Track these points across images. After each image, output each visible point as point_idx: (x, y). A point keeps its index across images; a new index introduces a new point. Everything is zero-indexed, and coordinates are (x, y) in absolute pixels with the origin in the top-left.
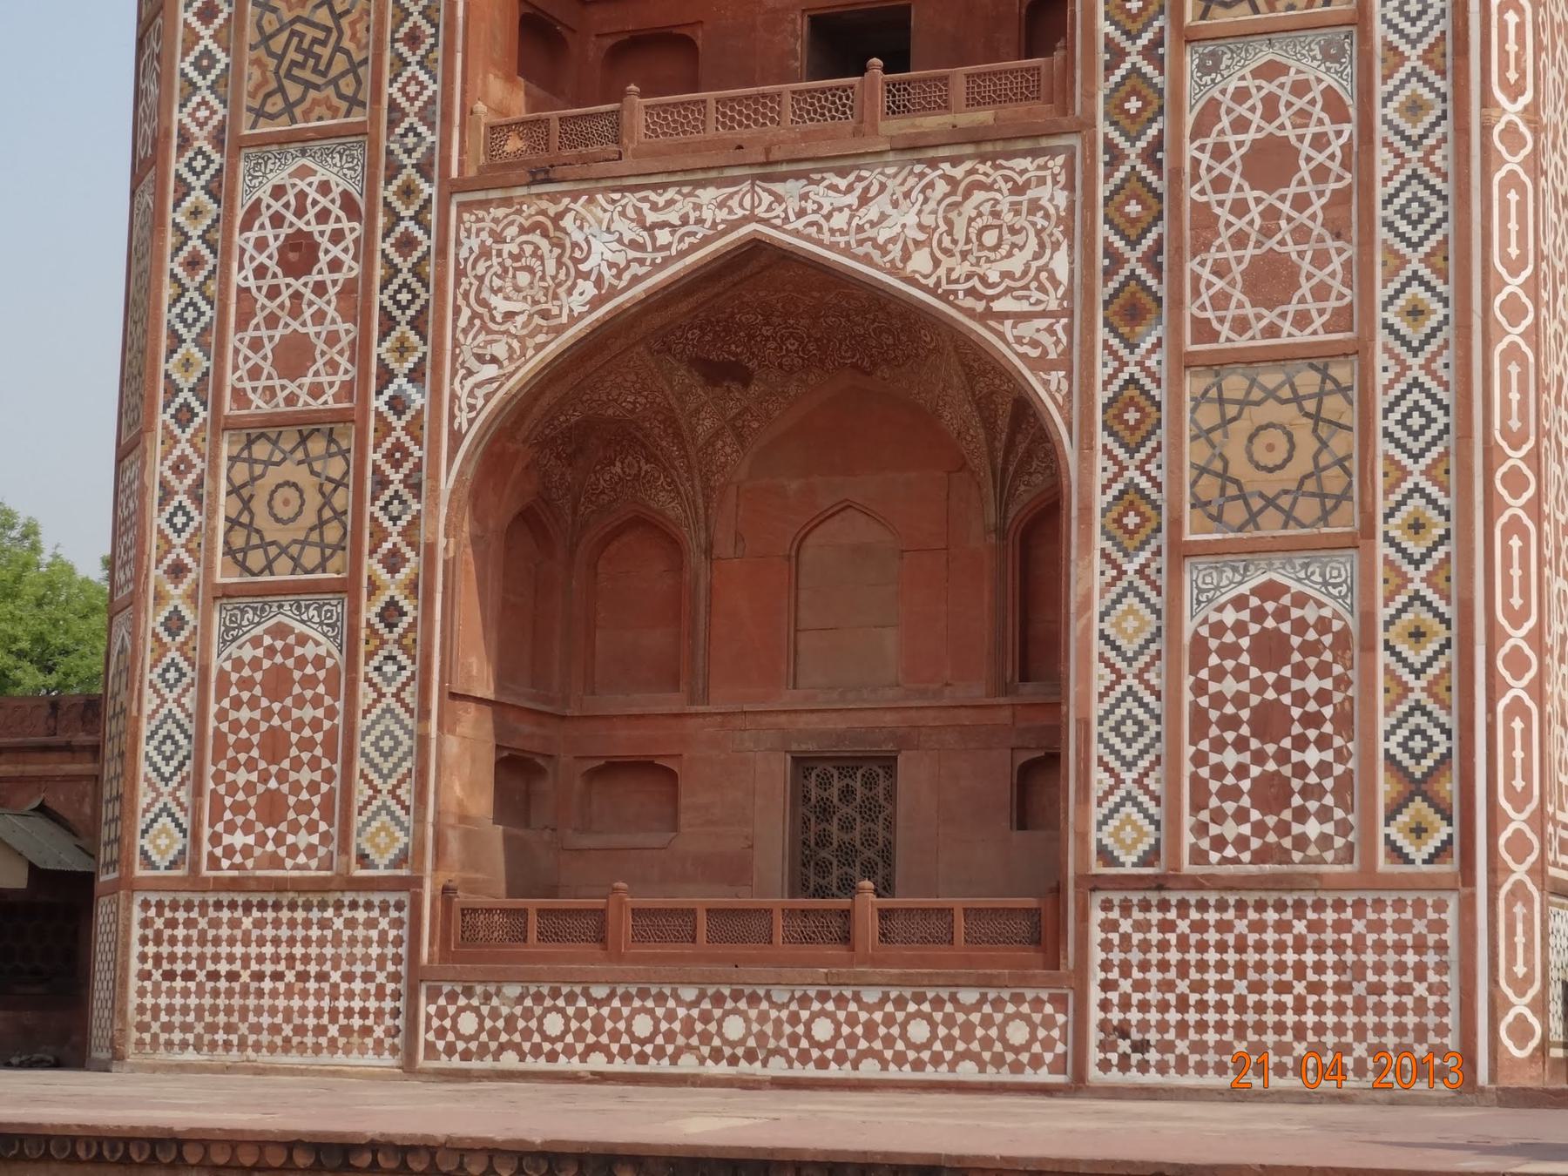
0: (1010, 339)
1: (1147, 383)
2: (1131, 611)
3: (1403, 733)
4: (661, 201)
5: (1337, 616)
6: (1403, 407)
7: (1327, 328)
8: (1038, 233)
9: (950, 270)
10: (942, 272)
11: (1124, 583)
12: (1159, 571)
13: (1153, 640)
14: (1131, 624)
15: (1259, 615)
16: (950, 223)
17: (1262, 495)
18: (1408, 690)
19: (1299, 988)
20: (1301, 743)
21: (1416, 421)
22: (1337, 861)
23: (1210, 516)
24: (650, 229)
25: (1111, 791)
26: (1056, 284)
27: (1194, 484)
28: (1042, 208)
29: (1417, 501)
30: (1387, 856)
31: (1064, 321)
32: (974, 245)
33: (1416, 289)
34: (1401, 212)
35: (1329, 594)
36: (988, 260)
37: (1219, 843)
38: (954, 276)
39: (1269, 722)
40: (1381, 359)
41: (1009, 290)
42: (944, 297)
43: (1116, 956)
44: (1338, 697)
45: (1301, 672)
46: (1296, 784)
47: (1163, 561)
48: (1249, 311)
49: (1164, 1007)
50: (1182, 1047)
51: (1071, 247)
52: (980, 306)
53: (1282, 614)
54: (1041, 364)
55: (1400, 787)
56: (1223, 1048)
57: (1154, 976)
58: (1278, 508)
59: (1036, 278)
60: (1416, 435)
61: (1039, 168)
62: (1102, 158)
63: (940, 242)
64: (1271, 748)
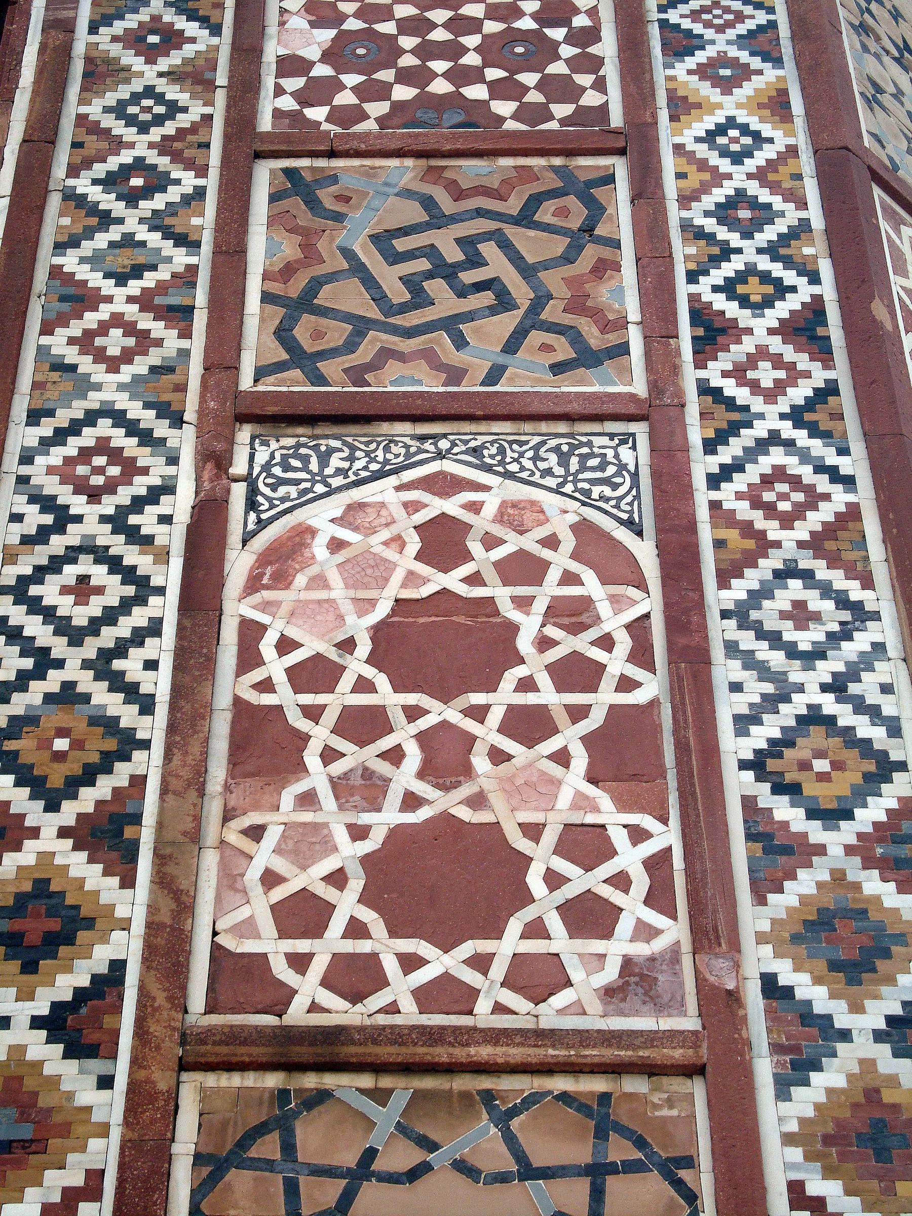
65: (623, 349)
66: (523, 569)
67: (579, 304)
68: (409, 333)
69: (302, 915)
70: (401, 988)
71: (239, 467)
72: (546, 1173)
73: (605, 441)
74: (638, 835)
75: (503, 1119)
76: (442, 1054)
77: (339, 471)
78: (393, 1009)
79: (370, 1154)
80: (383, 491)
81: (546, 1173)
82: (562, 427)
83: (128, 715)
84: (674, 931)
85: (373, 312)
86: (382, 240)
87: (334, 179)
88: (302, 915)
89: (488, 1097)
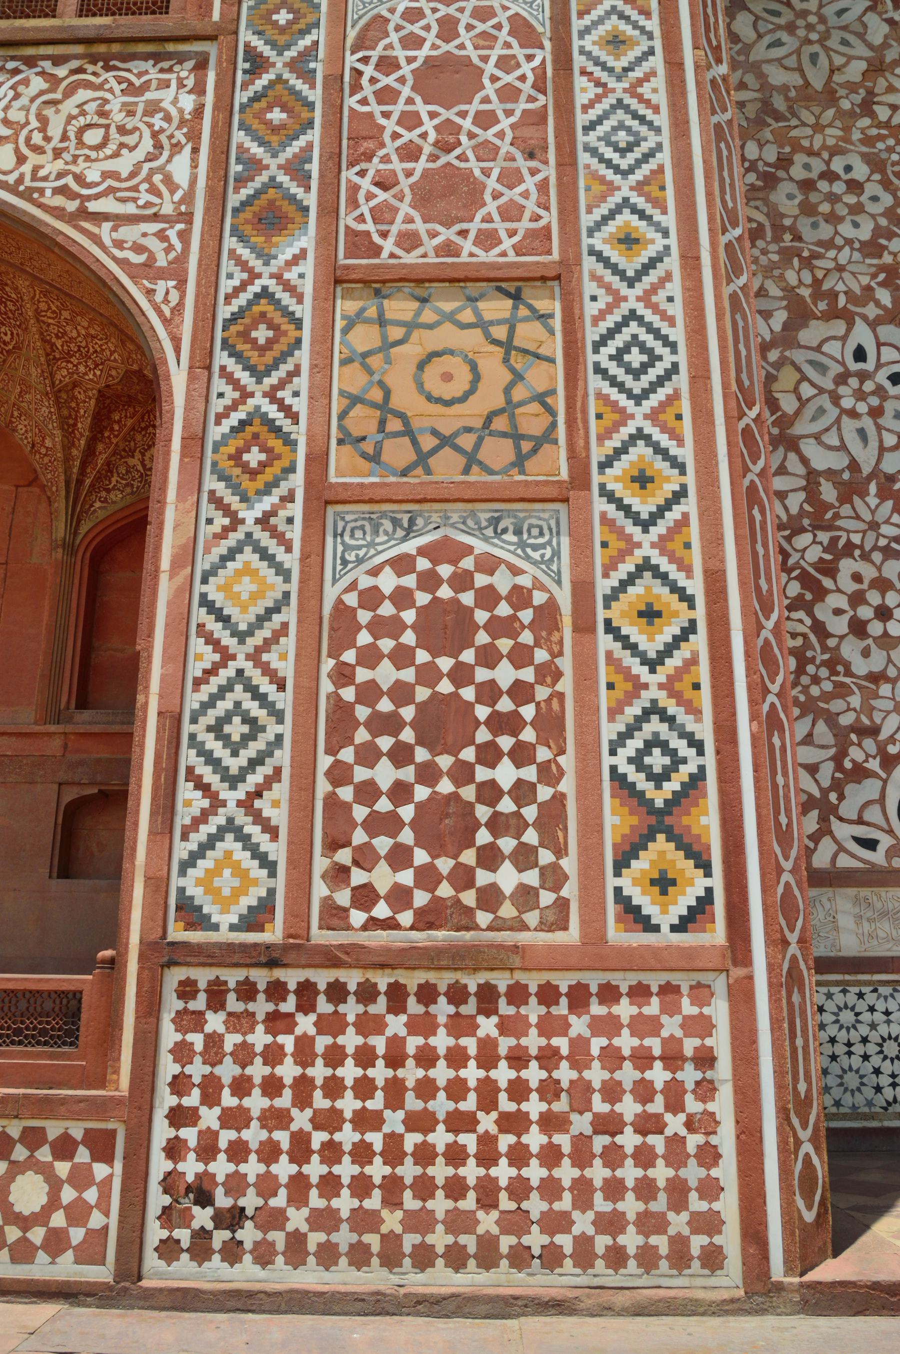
0: (107, 242)
1: (286, 298)
2: (248, 570)
3: (634, 744)
5: (538, 585)
6: (619, 341)
7: (518, 250)
8: (155, 135)
9: (36, 169)
10: (27, 168)
11: (240, 535)
12: (290, 521)
13: (278, 610)
14: (246, 587)
15: (429, 581)
16: (44, 122)
17: (435, 433)
18: (640, 686)
19: (487, 1122)
20: (490, 755)
21: (635, 358)
22: (545, 926)
23: (364, 456)
25: (204, 817)
26: (173, 187)
27: (342, 416)
28: (162, 110)
29: (641, 450)
30: (618, 920)
31: (180, 226)
32: (72, 144)
33: (626, 216)
34: (606, 139)
35: (528, 558)
36: (88, 158)
37: (365, 896)
38: (42, 173)
39: (442, 724)
40: (589, 288)
41: (111, 190)
42: (26, 195)
43: (197, 1070)
44: (542, 693)
45: (489, 657)
46: (483, 812)
47: (297, 509)
48: (420, 226)
49: (269, 1153)
50: (297, 1219)
51: (195, 150)
52: (72, 206)
53: (462, 581)
54: (147, 271)
55: (634, 820)
56: (364, 1221)
57: (256, 1102)
58: (457, 449)
59: (148, 179)
60: (636, 374)
62: (242, 65)
63: (28, 139)
64: (445, 762)
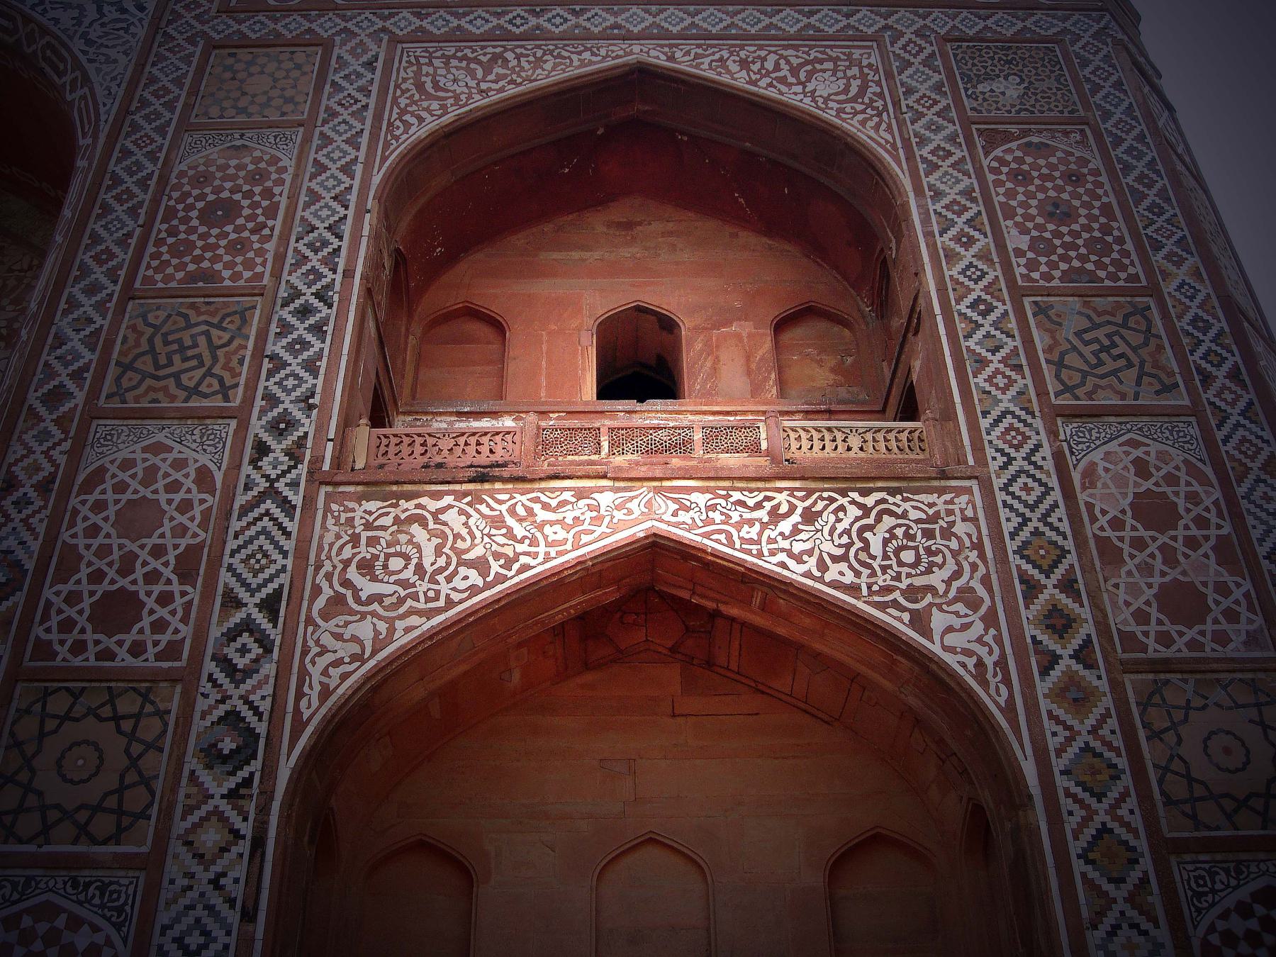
4: (554, 503)
24: (540, 527)
32: (894, 562)
61: (946, 502)
65: (1176, 385)
66: (1171, 480)
67: (1156, 365)
68: (1102, 377)
69: (1141, 617)
70: (1180, 643)
71: (1062, 437)
72: (1243, 706)
73: (1181, 425)
74: (1238, 585)
75: (1225, 688)
76: (1203, 667)
77: (1098, 438)
78: (1179, 650)
79: (1188, 701)
80: (1113, 447)
81: (1243, 706)
82: (1166, 419)
83: (1060, 540)
84: (1259, 621)
85: (1086, 368)
86: (1078, 334)
87: (1052, 307)
88: (1141, 617)
89: (1218, 680)
